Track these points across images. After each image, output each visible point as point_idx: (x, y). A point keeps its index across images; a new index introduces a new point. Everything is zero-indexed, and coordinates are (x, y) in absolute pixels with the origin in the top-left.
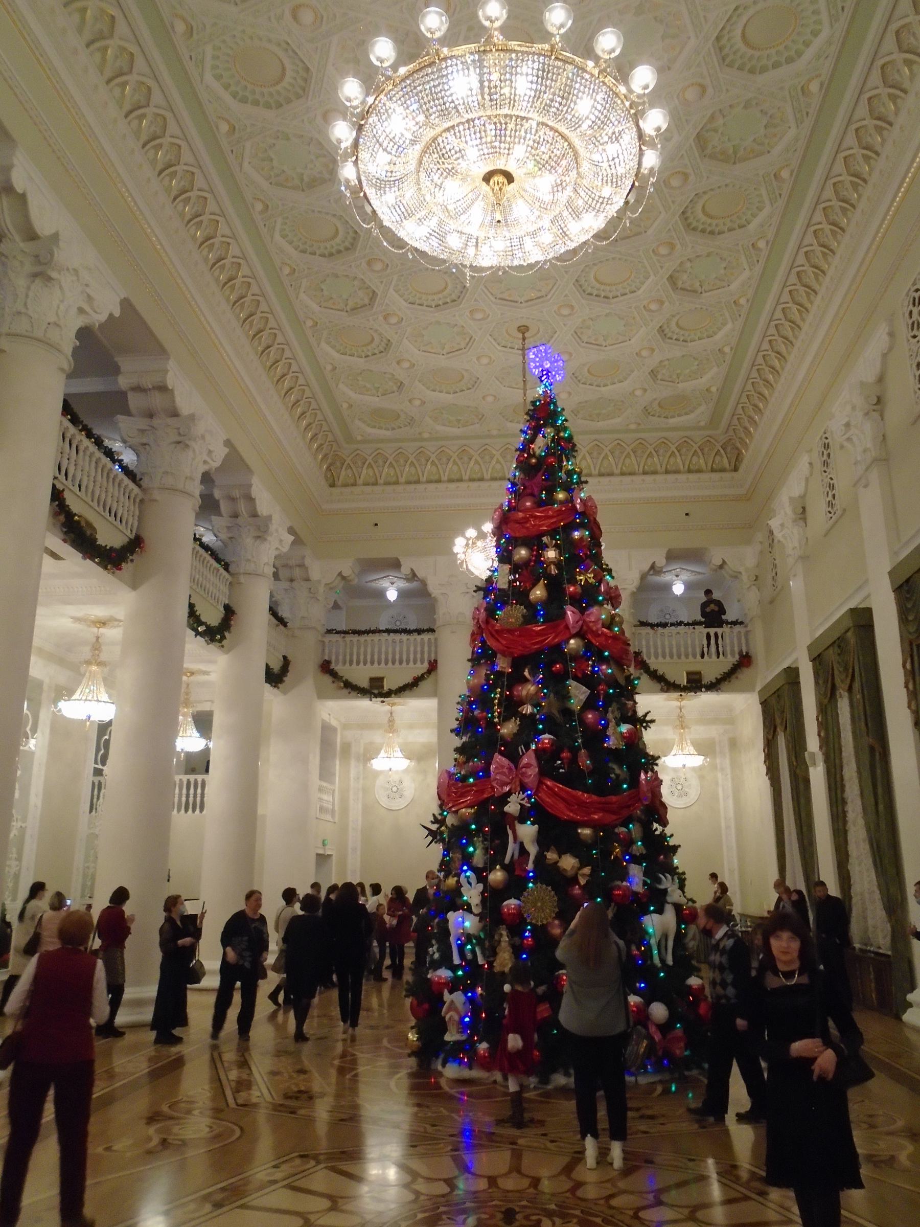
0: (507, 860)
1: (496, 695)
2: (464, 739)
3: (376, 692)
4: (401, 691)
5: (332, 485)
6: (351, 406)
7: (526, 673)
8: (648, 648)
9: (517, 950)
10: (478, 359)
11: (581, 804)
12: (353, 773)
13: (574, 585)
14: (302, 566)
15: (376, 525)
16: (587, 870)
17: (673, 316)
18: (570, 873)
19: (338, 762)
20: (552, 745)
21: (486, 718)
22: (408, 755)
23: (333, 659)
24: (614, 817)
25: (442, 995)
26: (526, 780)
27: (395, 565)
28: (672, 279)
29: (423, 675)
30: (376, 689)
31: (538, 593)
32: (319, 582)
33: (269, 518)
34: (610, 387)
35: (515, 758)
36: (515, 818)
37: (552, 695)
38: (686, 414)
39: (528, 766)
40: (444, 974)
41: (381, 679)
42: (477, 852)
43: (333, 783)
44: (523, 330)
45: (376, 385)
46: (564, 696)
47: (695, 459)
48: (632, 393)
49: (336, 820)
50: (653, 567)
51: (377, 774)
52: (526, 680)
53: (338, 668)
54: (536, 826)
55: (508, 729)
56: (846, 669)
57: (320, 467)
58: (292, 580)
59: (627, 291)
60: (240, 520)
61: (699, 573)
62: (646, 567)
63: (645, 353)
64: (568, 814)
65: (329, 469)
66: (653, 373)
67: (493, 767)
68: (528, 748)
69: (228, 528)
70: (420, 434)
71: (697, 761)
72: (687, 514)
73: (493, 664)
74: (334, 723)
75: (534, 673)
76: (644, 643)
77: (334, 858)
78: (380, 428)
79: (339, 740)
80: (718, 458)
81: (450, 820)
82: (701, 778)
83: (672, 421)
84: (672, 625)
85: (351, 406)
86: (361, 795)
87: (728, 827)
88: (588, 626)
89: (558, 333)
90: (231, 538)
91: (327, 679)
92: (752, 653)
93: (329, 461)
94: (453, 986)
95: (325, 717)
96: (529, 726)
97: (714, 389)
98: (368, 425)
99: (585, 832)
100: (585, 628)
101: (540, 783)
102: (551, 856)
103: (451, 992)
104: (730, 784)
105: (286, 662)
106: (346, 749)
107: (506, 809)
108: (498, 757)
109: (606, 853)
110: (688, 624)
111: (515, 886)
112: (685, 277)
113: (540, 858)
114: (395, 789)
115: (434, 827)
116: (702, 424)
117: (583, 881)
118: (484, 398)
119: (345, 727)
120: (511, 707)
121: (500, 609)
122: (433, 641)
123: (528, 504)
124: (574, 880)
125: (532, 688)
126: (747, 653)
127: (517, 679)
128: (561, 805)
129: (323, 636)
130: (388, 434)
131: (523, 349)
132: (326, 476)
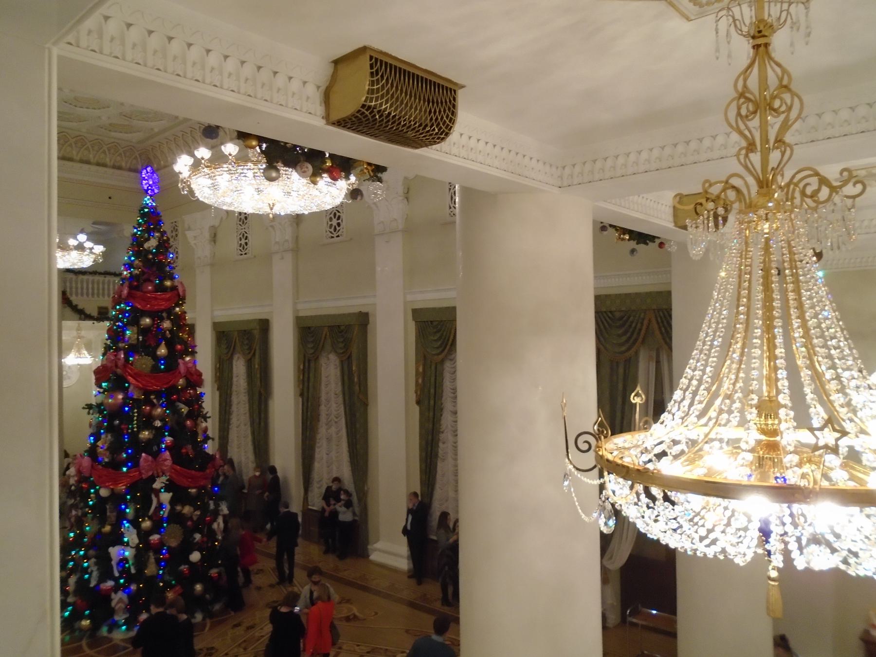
8: (71, 288)
9: (158, 562)
16: (198, 513)
25: (110, 596)
31: (162, 351)
38: (126, 133)
40: (110, 583)
54: (171, 494)
55: (145, 434)
56: (250, 349)
94: (116, 588)
96: (159, 434)
102: (179, 508)
103: (116, 592)
110: (100, 274)
111: (157, 527)
113: (172, 509)
117: (195, 518)
124: (191, 519)
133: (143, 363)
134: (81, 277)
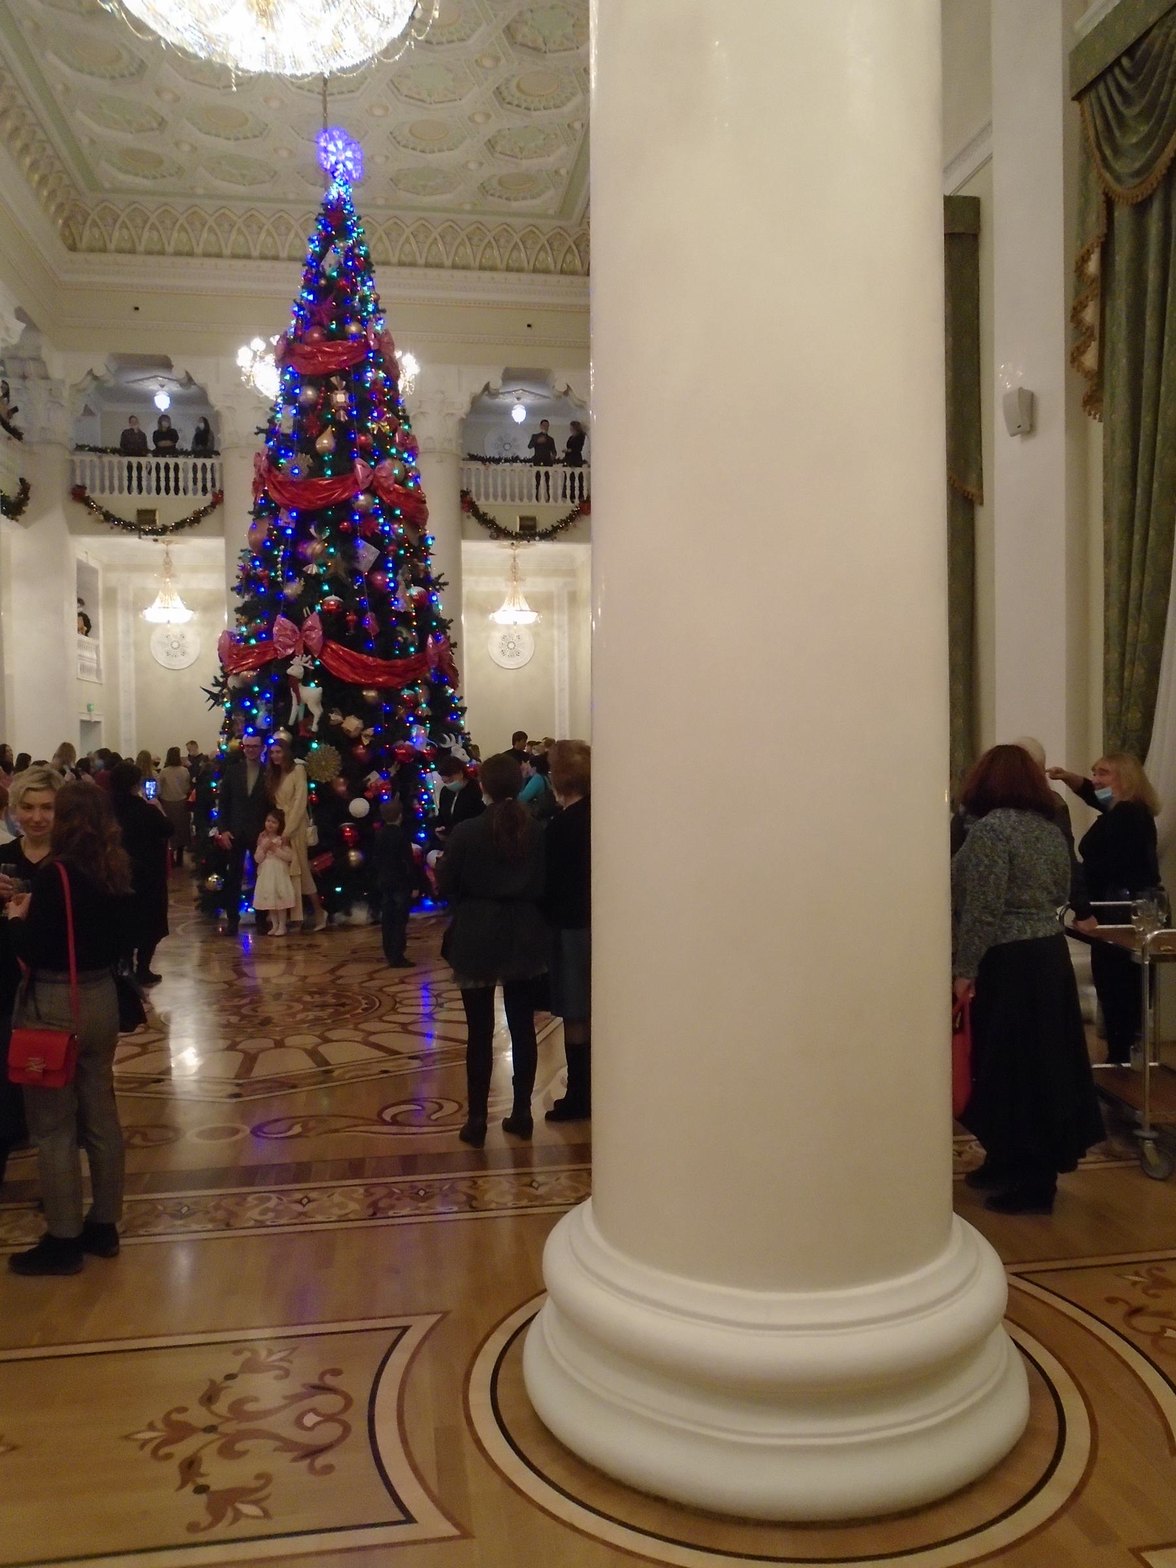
0: (291, 722)
1: (278, 553)
2: (247, 598)
3: (148, 528)
4: (179, 526)
5: (73, 248)
6: (93, 142)
7: (312, 530)
8: (478, 486)
10: (266, 100)
11: (366, 666)
12: (121, 626)
13: (364, 435)
14: (37, 359)
15: (137, 309)
16: (370, 731)
17: (513, 76)
18: (354, 734)
19: (101, 612)
20: (338, 607)
21: (268, 577)
22: (191, 604)
23: (88, 483)
24: (398, 680)
26: (310, 643)
27: (165, 364)
28: (509, 31)
30: (144, 523)
31: (325, 442)
32: (63, 382)
34: (437, 155)
35: (299, 620)
36: (299, 680)
37: (339, 555)
38: (533, 197)
39: (312, 628)
41: (152, 512)
42: (260, 713)
43: (97, 637)
46: (351, 556)
47: (542, 255)
48: (465, 166)
49: (104, 681)
50: (487, 388)
51: (152, 627)
52: (312, 538)
53: (95, 495)
55: (292, 589)
57: (54, 222)
58: (24, 377)
59: (455, 38)
61: (545, 397)
62: (478, 388)
63: (479, 119)
64: (351, 677)
65: (66, 224)
66: (491, 144)
67: (275, 629)
68: (312, 610)
70: (192, 188)
71: (531, 617)
73: (276, 518)
74: (93, 563)
75: (320, 530)
76: (473, 480)
77: (103, 724)
79: (100, 585)
80: (569, 258)
81: (232, 682)
82: (536, 635)
83: (515, 205)
84: (507, 461)
86: (132, 650)
87: (561, 690)
88: (379, 482)
89: (369, 80)
91: (81, 508)
93: (66, 214)
95: (82, 557)
97: (563, 172)
98: (120, 169)
99: (371, 694)
100: (375, 484)
101: (325, 646)
102: (335, 717)
104: (566, 643)
105: (25, 487)
107: (289, 671)
108: (281, 620)
109: (390, 715)
112: (526, 30)
113: (324, 719)
114: (175, 645)
115: (216, 690)
116: (551, 212)
117: (366, 742)
118: (275, 150)
119: (108, 568)
120: (295, 563)
121: (285, 456)
123: (316, 335)
124: (358, 740)
125: (317, 547)
127: (302, 535)
128: (346, 669)
129: (72, 453)
130: (148, 183)
131: (324, 94)
132: (63, 235)
133: (295, 465)
134: (493, 466)
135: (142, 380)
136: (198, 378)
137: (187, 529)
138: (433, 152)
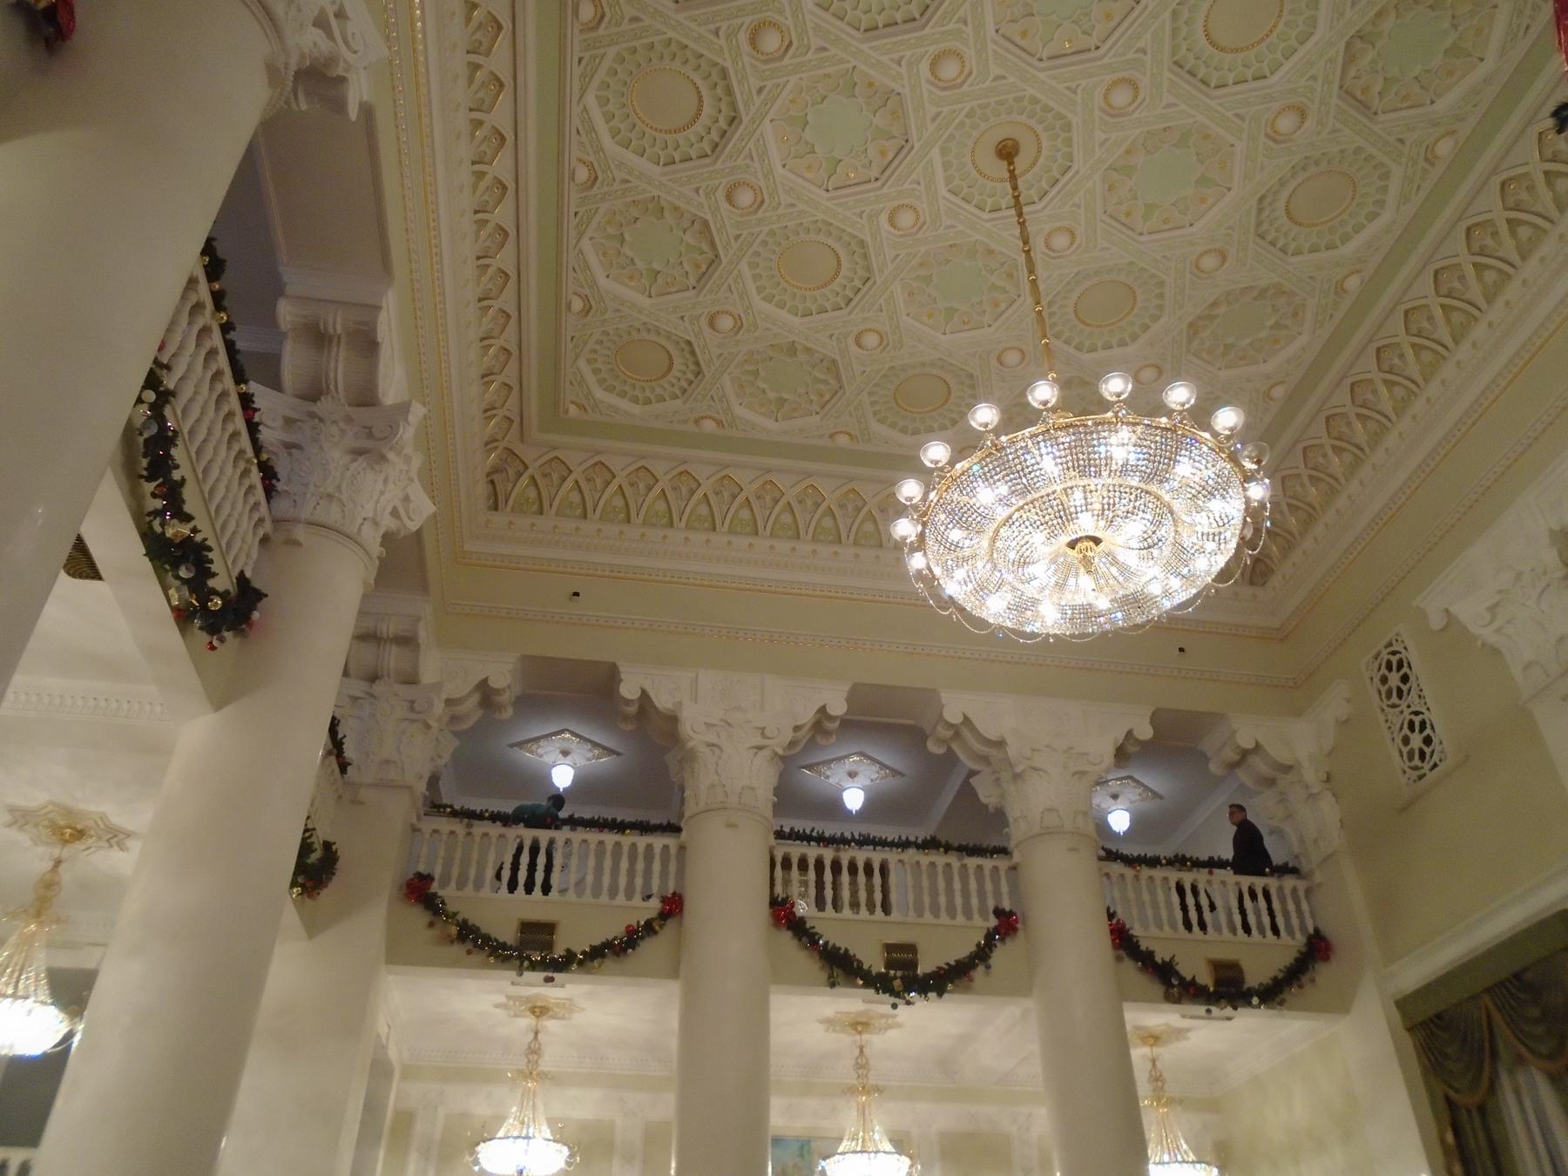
14: (407, 641)
19: (381, 1155)
23: (437, 872)
29: (649, 924)
30: (536, 950)
33: (404, 409)
41: (549, 928)
44: (1007, 152)
45: (656, 266)
53: (448, 893)
60: (323, 406)
69: (289, 422)
72: (1181, 650)
78: (623, 394)
85: (587, 310)
90: (289, 446)
91: (417, 917)
92: (1326, 931)
98: (601, 382)
106: (405, 1121)
119: (409, 1073)
122: (673, 851)
126: (1317, 930)
134: (1146, 872)
135: (536, 740)
136: (663, 701)
137: (609, 963)
138: (1093, 349)
